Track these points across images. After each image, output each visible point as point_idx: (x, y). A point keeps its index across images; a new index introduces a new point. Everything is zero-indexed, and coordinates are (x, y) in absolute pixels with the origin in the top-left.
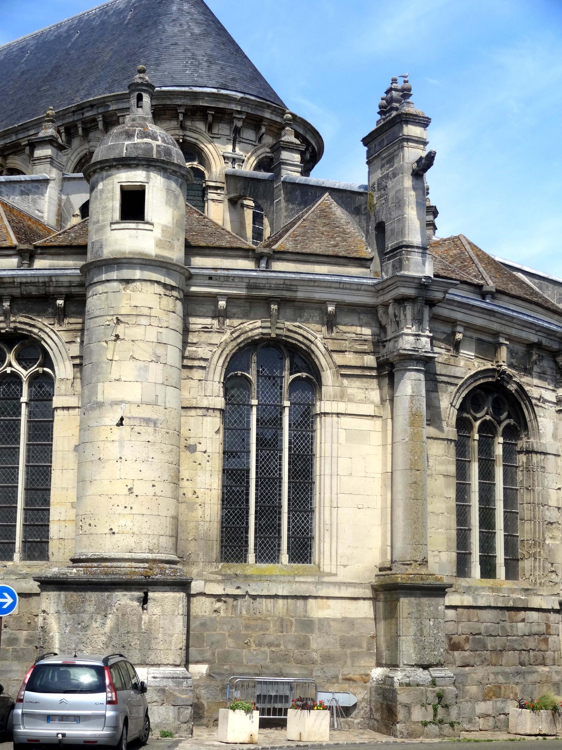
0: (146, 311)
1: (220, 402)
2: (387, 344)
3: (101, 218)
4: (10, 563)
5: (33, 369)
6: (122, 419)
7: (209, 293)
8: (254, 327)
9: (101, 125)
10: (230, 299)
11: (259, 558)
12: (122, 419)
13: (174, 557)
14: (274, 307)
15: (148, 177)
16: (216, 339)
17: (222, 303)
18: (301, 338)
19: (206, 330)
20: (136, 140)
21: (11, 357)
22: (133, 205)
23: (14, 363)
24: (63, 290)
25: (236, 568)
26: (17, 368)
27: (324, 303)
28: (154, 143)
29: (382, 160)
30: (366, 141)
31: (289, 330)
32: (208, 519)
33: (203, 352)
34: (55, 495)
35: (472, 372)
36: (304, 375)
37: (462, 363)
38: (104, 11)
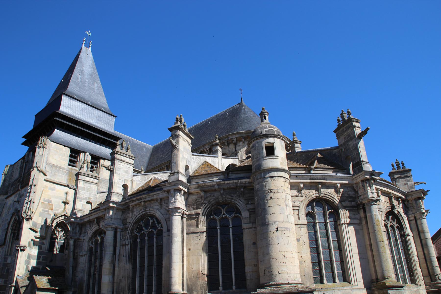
0: (280, 188)
1: (305, 222)
2: (360, 197)
3: (258, 156)
4: (231, 290)
5: (233, 215)
6: (277, 228)
7: (297, 182)
8: (313, 194)
9: (226, 144)
10: (304, 184)
11: (328, 282)
12: (277, 228)
13: (301, 282)
14: (320, 186)
15: (274, 140)
16: (301, 199)
17: (302, 185)
18: (330, 197)
19: (296, 196)
20: (268, 129)
21: (224, 211)
22: (271, 151)
23: (225, 213)
24: (243, 185)
25: (320, 286)
26: (227, 215)
27: (337, 183)
28: (275, 130)
30: (335, 132)
31: (325, 194)
32: (308, 267)
33: (297, 204)
34: (247, 262)
35: (385, 207)
36: (332, 210)
37: (382, 204)
38: (217, 116)
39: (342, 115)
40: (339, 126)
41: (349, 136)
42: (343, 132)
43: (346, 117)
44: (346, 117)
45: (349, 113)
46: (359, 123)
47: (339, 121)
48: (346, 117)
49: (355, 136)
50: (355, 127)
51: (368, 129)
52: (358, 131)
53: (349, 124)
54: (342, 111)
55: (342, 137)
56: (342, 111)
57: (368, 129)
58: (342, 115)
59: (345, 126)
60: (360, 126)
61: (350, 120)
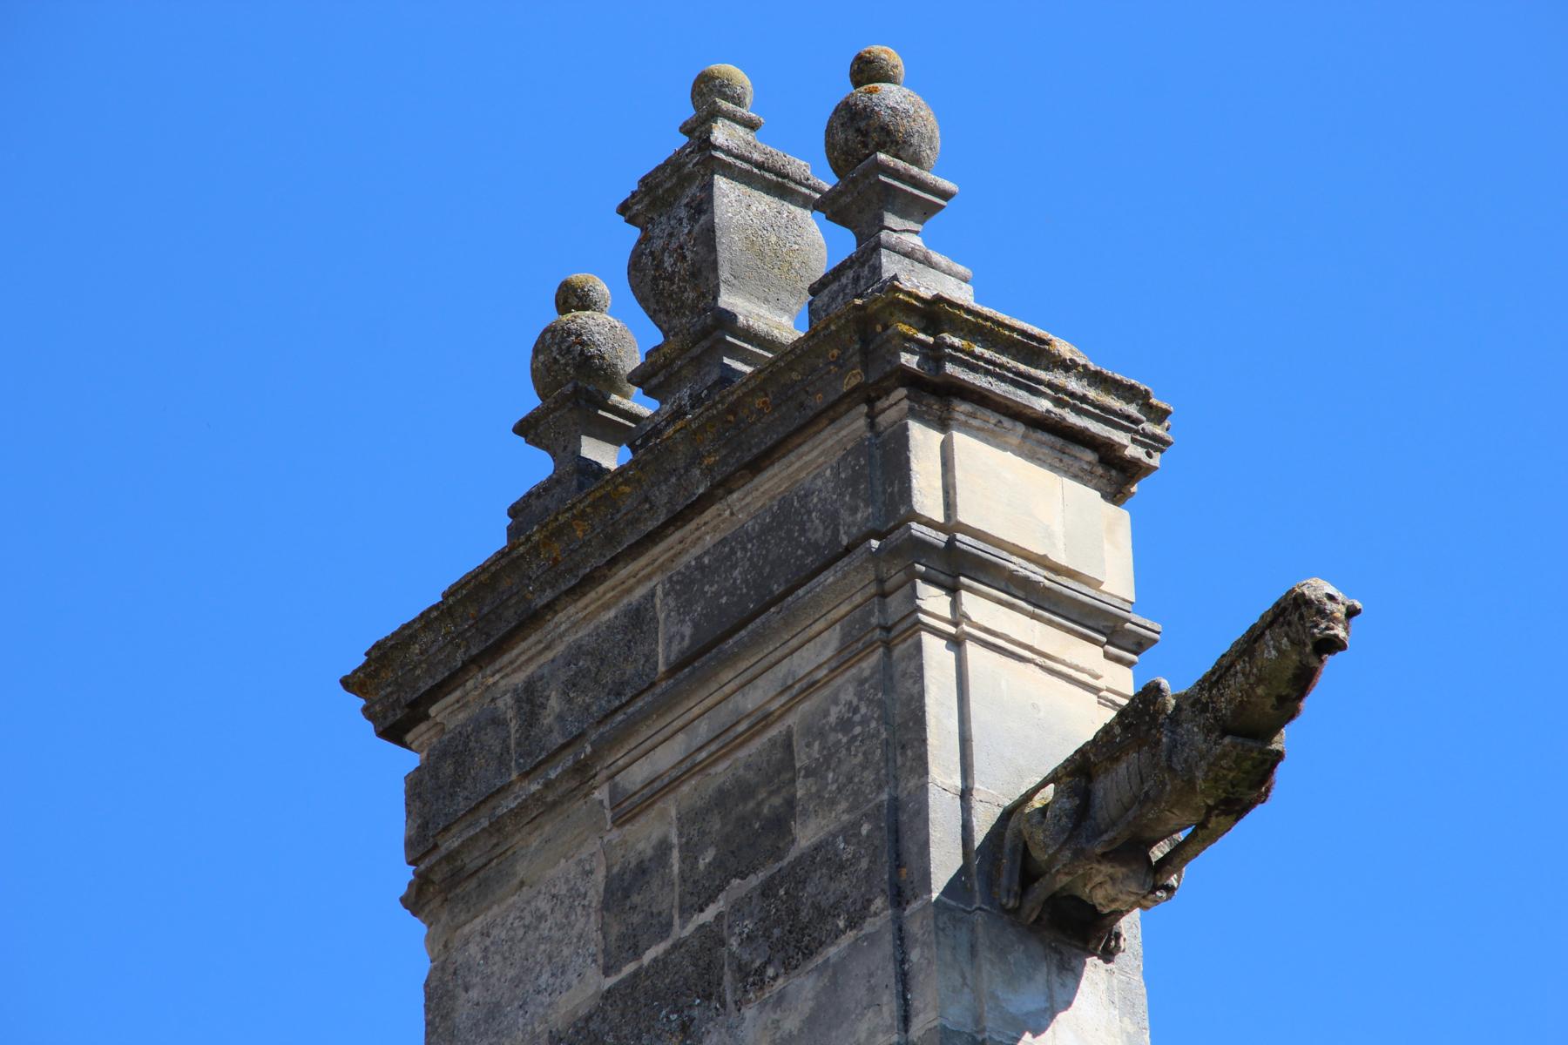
29: (627, 810)
30: (396, 687)
39: (670, 211)
40: (560, 539)
41: (748, 828)
42: (626, 694)
43: (768, 266)
44: (774, 267)
45: (866, 170)
46: (1116, 475)
47: (570, 384)
48: (774, 267)
49: (901, 827)
50: (959, 563)
51: (1289, 648)
52: (1012, 714)
53: (813, 463)
54: (709, 93)
55: (563, 867)
56: (709, 93)
57: (1289, 648)
58: (670, 211)
59: (702, 537)
60: (1114, 575)
61: (887, 361)
